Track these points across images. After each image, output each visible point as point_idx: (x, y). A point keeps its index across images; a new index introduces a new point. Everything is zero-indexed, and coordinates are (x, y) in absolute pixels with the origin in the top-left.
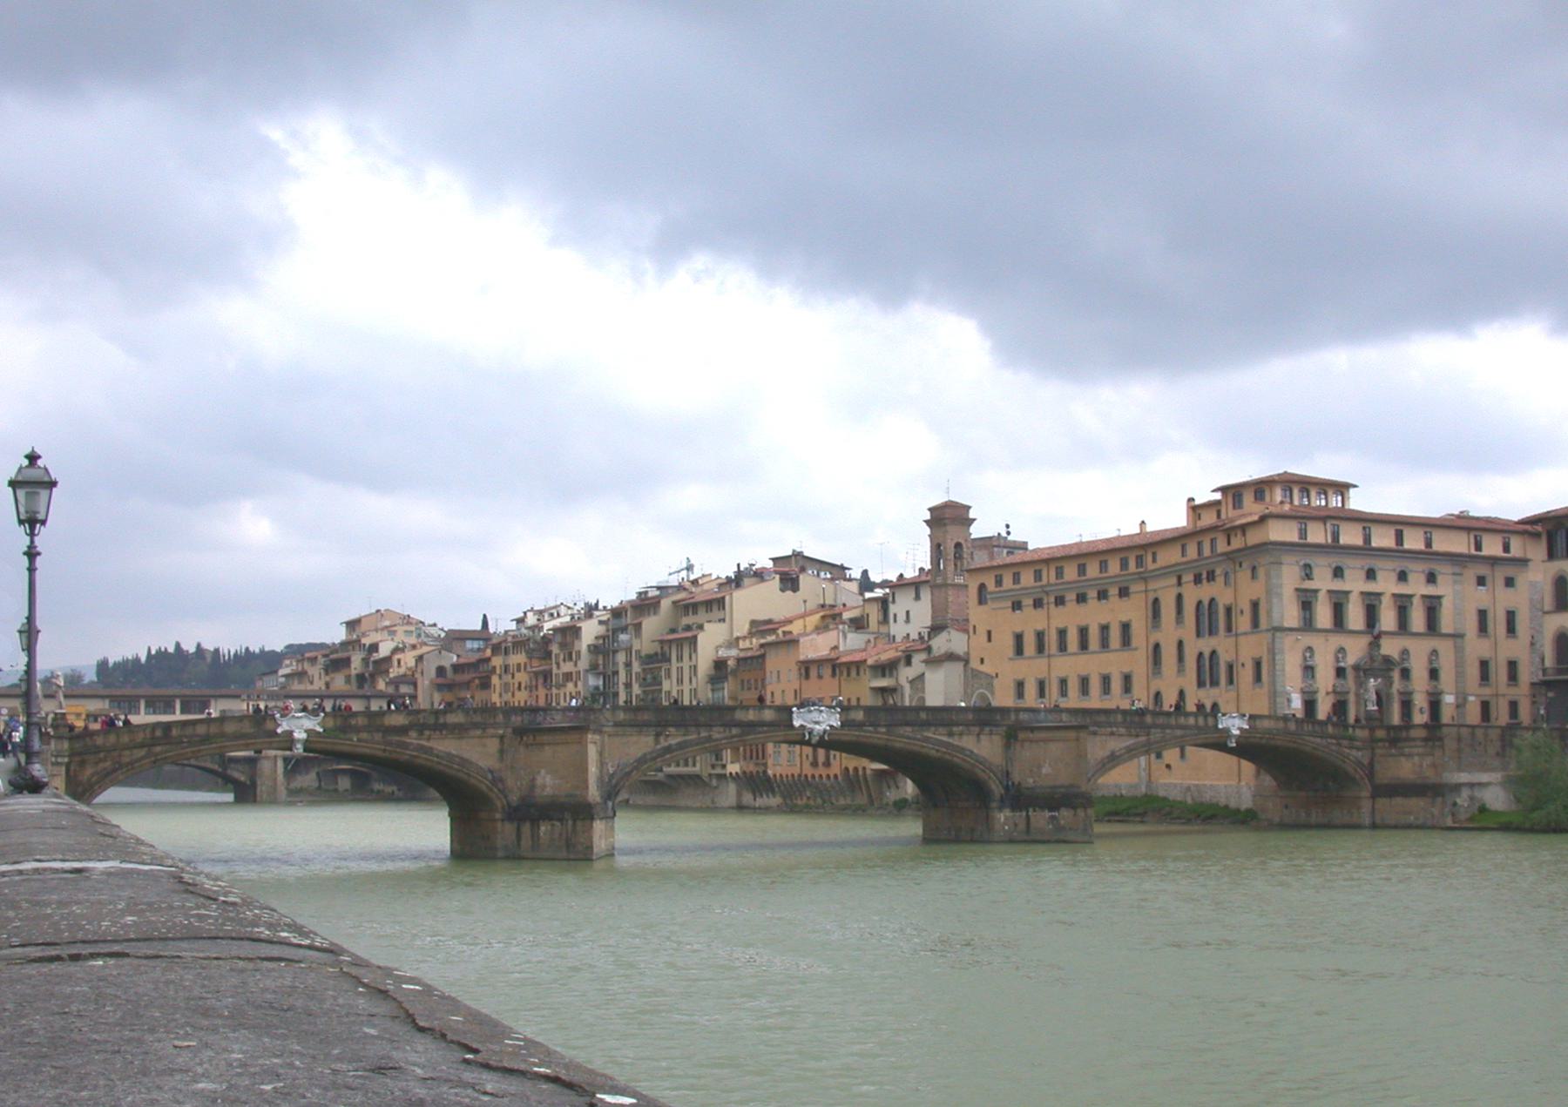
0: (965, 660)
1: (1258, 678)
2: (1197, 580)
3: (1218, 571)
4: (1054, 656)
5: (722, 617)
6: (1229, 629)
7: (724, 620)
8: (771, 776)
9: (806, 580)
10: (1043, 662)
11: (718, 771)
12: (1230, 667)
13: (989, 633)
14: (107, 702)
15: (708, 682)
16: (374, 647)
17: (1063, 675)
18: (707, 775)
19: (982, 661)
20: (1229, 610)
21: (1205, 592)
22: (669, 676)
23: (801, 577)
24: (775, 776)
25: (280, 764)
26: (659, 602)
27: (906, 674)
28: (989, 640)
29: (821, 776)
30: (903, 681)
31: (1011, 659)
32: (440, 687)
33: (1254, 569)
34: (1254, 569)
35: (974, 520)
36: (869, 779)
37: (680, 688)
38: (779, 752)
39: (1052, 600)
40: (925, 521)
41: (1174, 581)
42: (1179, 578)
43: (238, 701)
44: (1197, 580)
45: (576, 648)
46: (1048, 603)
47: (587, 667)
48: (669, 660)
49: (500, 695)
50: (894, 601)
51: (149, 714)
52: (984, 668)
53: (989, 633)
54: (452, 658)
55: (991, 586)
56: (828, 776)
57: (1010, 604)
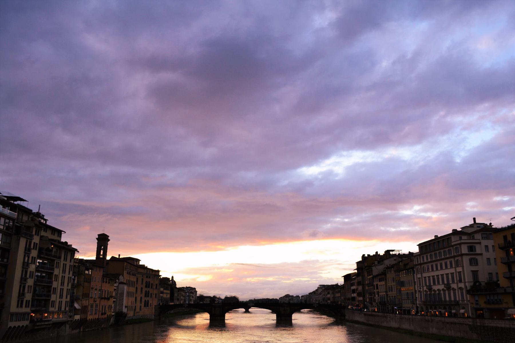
1: (156, 297)
2: (147, 277)
3: (151, 277)
6: (152, 287)
8: (88, 320)
12: (151, 294)
20: (152, 284)
21: (148, 280)
22: (58, 267)
24: (89, 319)
29: (103, 318)
33: (157, 279)
34: (157, 279)
38: (93, 309)
41: (142, 276)
42: (143, 275)
44: (147, 277)
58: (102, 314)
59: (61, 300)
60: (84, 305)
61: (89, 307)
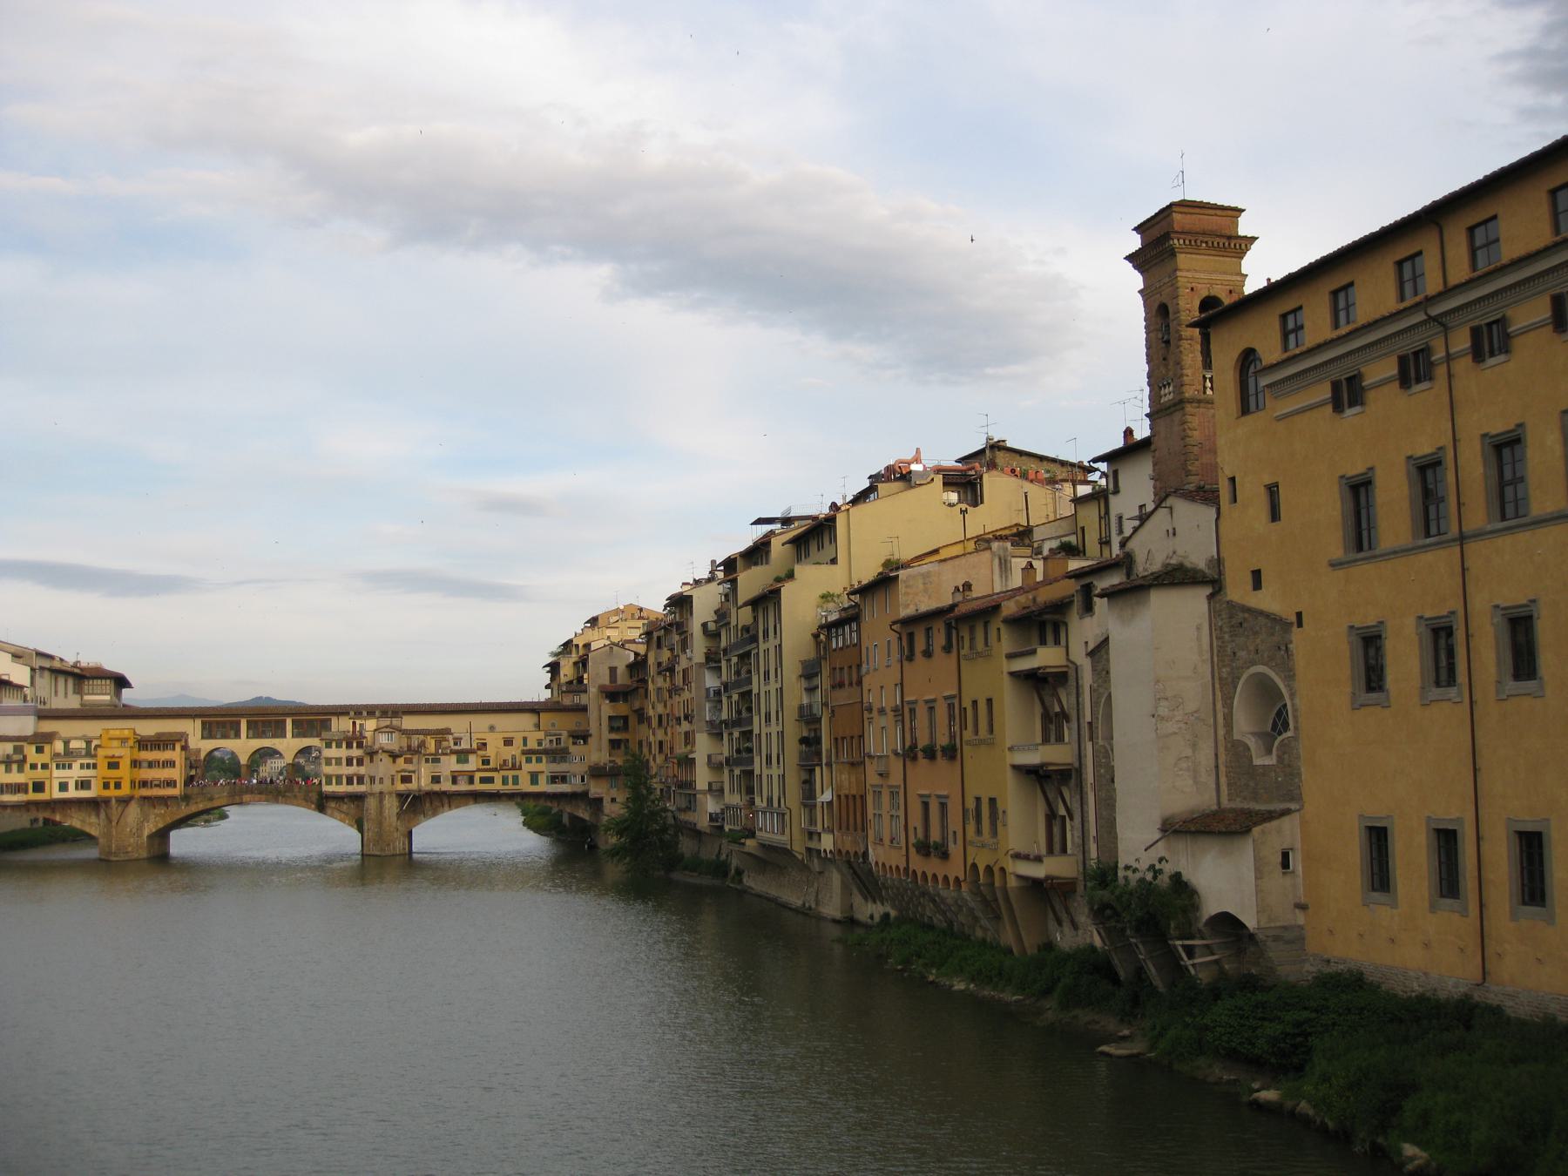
0: (1211, 580)
4: (1479, 535)
5: (834, 556)
7: (834, 561)
9: (995, 485)
10: (1441, 562)
11: (813, 845)
13: (1273, 491)
14: (198, 722)
15: (800, 676)
16: (587, 646)
17: (1513, 596)
18: (804, 852)
19: (1257, 578)
23: (986, 477)
25: (391, 806)
26: (768, 543)
27: (1083, 631)
28: (1275, 515)
30: (1079, 656)
31: (1334, 565)
32: (612, 695)
35: (1254, 239)
36: (1012, 895)
37: (767, 688)
39: (1461, 341)
40: (1130, 258)
43: (347, 718)
45: (690, 632)
46: (1449, 358)
47: (703, 660)
48: (754, 639)
49: (653, 708)
50: (1116, 491)
51: (254, 737)
52: (1267, 600)
53: (1273, 491)
54: (629, 656)
55: (1270, 351)
56: (946, 878)
57: (1324, 392)
58: (924, 848)
59: (770, 772)
60: (844, 792)
61: (870, 799)
